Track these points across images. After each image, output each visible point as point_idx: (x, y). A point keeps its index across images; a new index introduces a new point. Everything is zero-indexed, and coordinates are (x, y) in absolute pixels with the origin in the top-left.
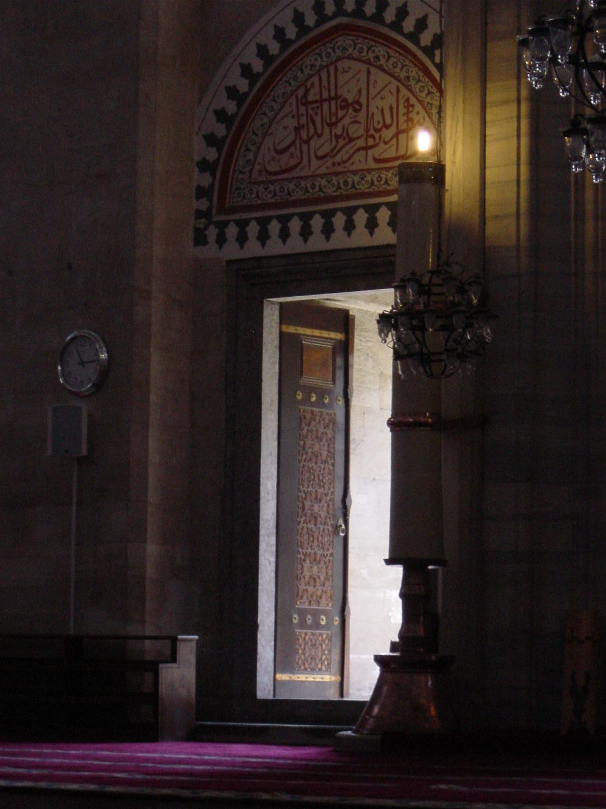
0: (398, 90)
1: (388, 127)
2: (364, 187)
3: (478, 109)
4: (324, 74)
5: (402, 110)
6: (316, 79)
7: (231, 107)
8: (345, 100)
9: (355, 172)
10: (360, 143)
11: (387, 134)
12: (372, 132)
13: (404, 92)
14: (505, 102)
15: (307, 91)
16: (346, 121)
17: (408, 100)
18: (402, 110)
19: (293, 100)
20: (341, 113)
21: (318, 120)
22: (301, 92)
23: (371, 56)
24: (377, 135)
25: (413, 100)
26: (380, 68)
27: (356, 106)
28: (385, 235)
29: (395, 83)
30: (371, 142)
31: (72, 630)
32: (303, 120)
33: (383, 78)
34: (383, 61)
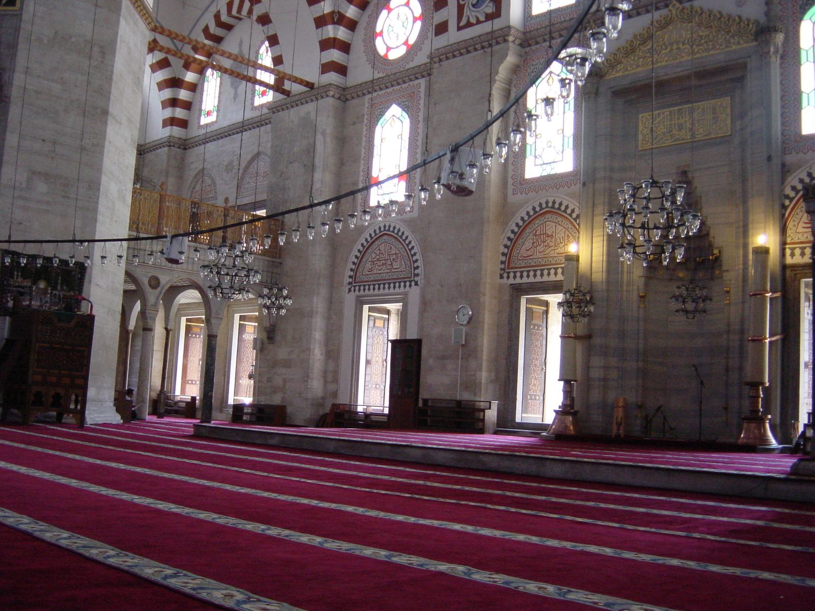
2: (553, 262)
3: (590, 238)
4: (542, 226)
6: (539, 228)
7: (512, 236)
9: (551, 257)
10: (553, 248)
11: (561, 245)
13: (567, 232)
14: (598, 236)
16: (548, 241)
20: (547, 238)
21: (539, 240)
22: (534, 232)
27: (552, 236)
28: (560, 277)
29: (564, 229)
31: (458, 399)
32: (535, 241)
33: (561, 228)
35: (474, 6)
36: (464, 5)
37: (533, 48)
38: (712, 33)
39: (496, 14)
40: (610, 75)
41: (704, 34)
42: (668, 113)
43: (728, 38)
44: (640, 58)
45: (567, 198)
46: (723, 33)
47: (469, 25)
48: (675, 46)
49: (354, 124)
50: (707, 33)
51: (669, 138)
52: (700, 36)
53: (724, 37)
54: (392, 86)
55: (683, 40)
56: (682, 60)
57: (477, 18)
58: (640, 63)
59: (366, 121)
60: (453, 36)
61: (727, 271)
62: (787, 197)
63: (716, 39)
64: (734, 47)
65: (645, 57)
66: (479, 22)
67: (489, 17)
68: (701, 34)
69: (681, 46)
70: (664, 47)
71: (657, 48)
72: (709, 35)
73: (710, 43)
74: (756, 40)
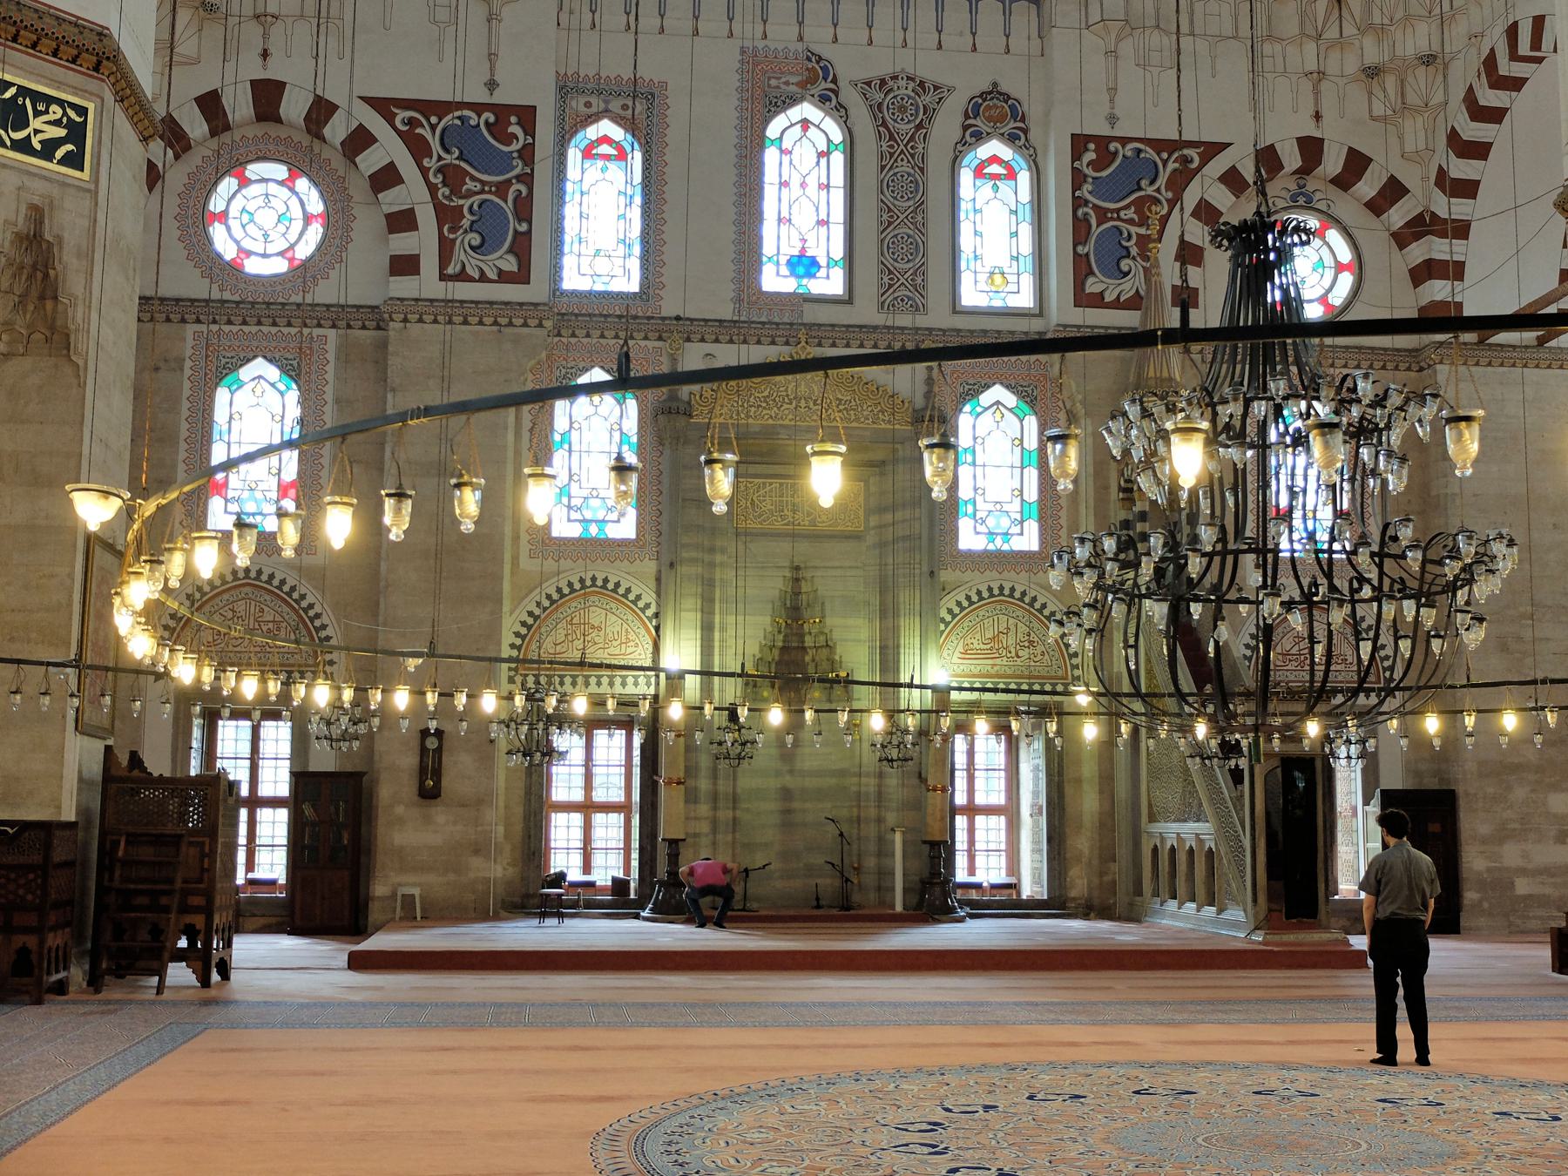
33: (614, 618)
35: (472, 248)
36: (454, 241)
39: (522, 276)
45: (630, 578)
47: (462, 276)
48: (803, 403)
49: (157, 369)
54: (259, 323)
57: (482, 272)
59: (188, 372)
60: (428, 283)
62: (942, 620)
64: (883, 426)
65: (759, 406)
66: (483, 278)
67: (504, 277)
68: (840, 396)
69: (811, 405)
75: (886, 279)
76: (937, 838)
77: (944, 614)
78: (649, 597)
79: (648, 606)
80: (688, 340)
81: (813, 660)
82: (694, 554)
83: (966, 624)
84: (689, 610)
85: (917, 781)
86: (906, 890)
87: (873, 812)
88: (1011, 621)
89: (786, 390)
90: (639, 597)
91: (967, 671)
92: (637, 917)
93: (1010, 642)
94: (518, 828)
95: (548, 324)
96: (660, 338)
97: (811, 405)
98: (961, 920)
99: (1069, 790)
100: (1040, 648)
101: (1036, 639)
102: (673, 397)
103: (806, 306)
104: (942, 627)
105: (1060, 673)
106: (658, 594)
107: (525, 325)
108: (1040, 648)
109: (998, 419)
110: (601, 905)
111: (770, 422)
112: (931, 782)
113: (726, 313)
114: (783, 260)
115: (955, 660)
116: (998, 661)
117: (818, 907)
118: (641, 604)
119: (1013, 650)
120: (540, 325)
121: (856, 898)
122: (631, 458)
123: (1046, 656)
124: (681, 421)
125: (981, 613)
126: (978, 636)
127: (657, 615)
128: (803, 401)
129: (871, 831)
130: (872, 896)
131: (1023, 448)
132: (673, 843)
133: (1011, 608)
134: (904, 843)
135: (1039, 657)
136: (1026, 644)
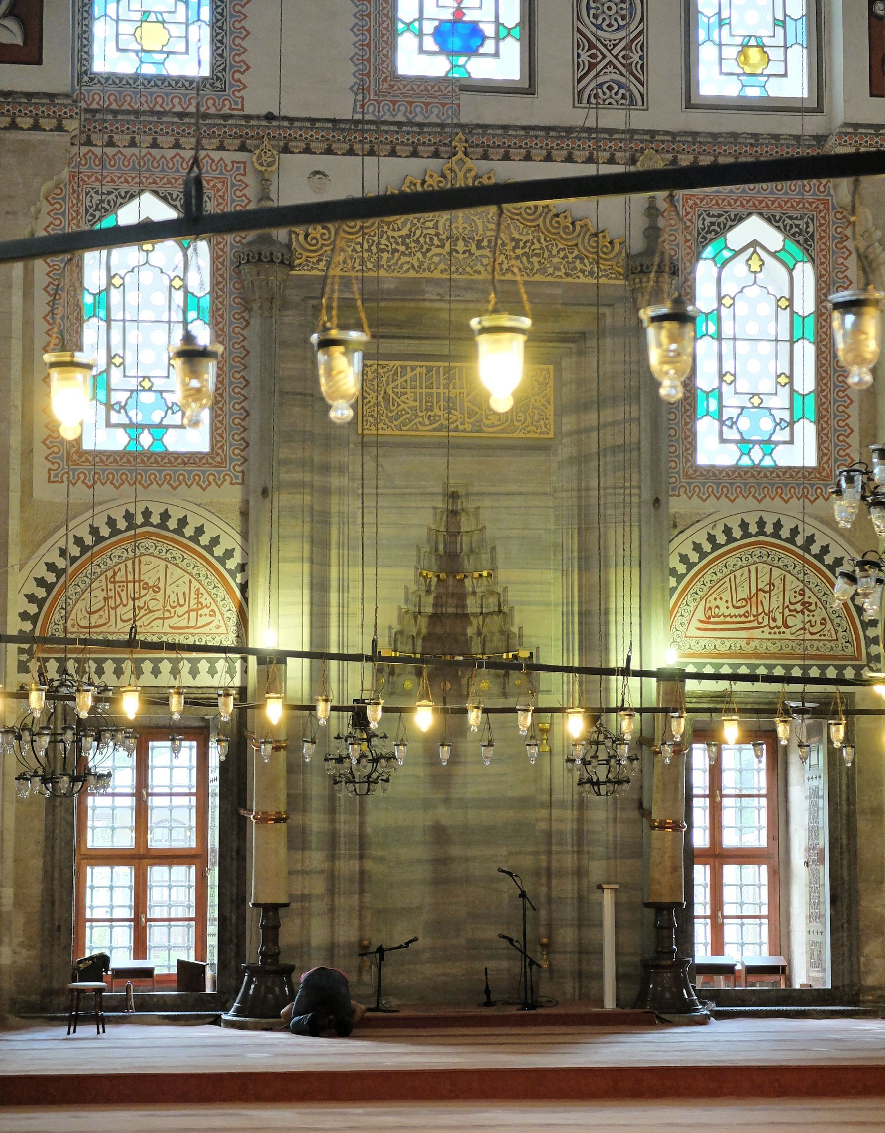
0: (190, 582)
1: (181, 606)
4: (130, 563)
5: (193, 596)
6: (122, 566)
8: (146, 583)
10: (158, 614)
11: (180, 611)
12: (168, 607)
13: (194, 582)
15: (115, 574)
16: (147, 598)
17: (198, 589)
18: (193, 596)
19: (103, 578)
20: (143, 592)
21: (124, 594)
22: (110, 574)
23: (169, 556)
24: (172, 611)
25: (202, 590)
26: (176, 565)
27: (156, 589)
30: (167, 614)
34: (178, 561)
37: (98, 151)
38: (539, 241)
40: (313, 268)
41: (524, 238)
42: (424, 370)
43: (571, 256)
44: (383, 251)
46: (560, 246)
50: (530, 237)
51: (427, 423)
52: (513, 239)
53: (562, 254)
55: (477, 238)
56: (476, 277)
58: (383, 262)
61: (548, 692)
62: (673, 572)
63: (546, 254)
64: (583, 280)
68: (516, 235)
69: (473, 248)
70: (436, 242)
71: (422, 240)
72: (533, 244)
73: (535, 259)
74: (626, 278)
75: (584, 56)
76: (667, 899)
77: (674, 562)
78: (231, 540)
79: (229, 554)
80: (286, 150)
81: (479, 634)
82: (297, 476)
83: (708, 578)
84: (293, 560)
85: (635, 814)
86: (619, 977)
87: (569, 862)
88: (776, 573)
89: (436, 226)
90: (215, 541)
91: (710, 648)
92: (216, 1021)
93: (774, 605)
94: (36, 889)
95: (72, 126)
96: (243, 148)
97: (473, 248)
98: (703, 1021)
99: (862, 825)
100: (820, 614)
101: (813, 600)
102: (267, 240)
103: (465, 98)
104: (673, 582)
105: (849, 650)
106: (245, 535)
107: (36, 127)
108: (820, 614)
109: (755, 267)
110: (161, 1004)
111: (412, 274)
112: (657, 816)
113: (344, 109)
114: (429, 27)
115: (692, 632)
116: (757, 633)
117: (489, 1003)
118: (219, 551)
119: (779, 617)
120: (59, 128)
121: (545, 989)
122: (203, 336)
123: (829, 625)
124: (276, 276)
125: (731, 562)
126: (726, 596)
127: (243, 567)
128: (461, 243)
129: (567, 887)
130: (569, 986)
131: (792, 312)
132: (271, 910)
133: (776, 553)
134: (617, 905)
135: (818, 627)
136: (799, 607)
